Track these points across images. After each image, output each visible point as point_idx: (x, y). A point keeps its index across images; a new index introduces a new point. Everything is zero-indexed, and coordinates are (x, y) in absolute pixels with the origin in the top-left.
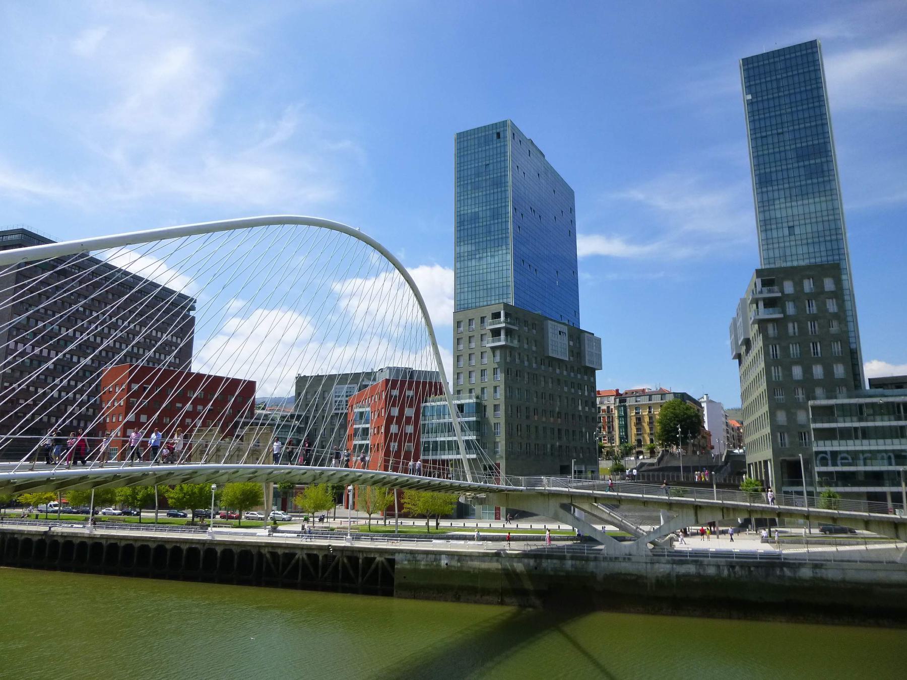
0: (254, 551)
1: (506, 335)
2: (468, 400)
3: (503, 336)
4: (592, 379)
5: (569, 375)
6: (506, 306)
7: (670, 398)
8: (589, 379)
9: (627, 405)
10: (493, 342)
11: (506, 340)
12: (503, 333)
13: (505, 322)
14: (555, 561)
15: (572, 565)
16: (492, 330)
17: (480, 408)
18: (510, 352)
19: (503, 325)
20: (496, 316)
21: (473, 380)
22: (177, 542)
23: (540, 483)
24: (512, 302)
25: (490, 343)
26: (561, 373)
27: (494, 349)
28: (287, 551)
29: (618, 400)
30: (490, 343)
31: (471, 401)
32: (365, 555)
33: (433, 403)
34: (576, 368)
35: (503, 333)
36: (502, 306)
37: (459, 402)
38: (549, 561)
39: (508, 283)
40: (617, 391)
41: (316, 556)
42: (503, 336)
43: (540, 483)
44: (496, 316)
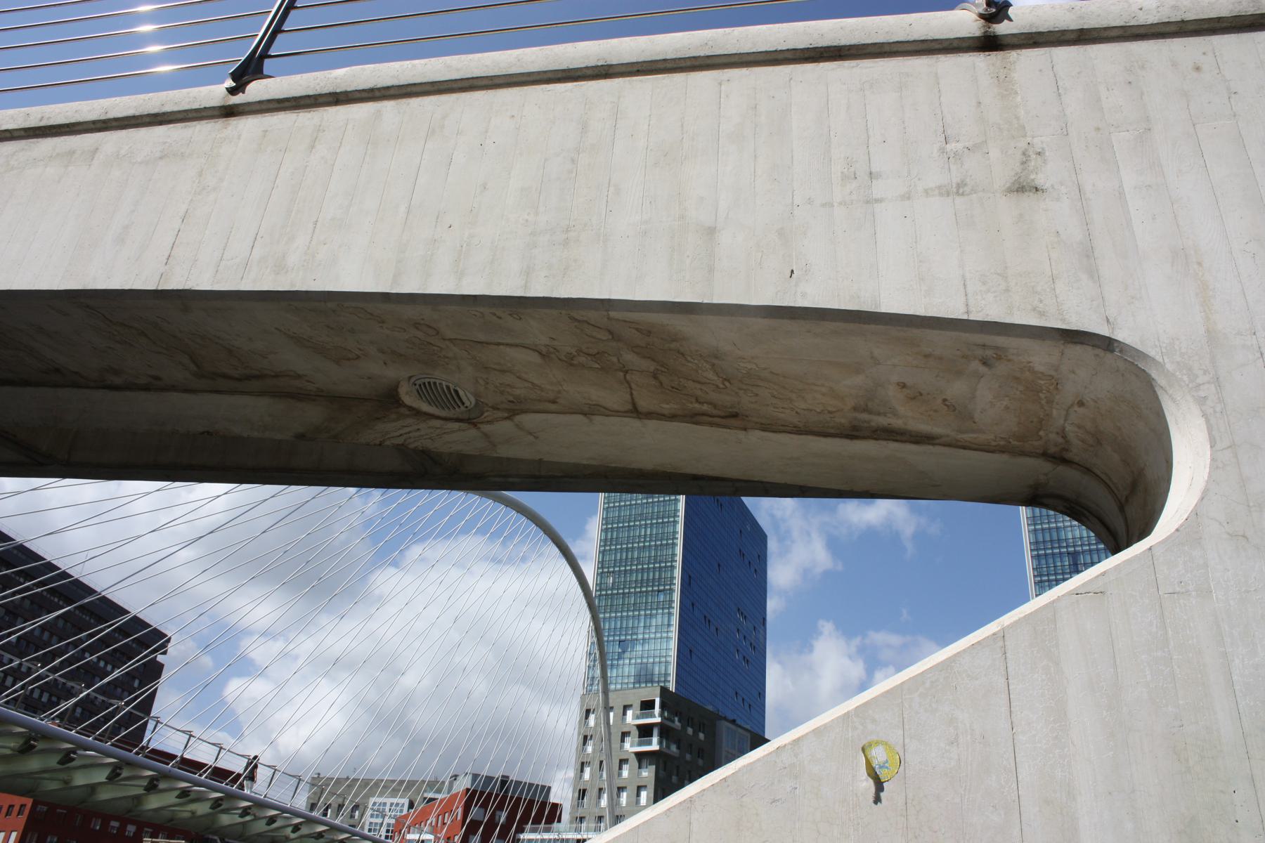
1: (661, 735)
3: (655, 739)
6: (664, 691)
10: (640, 744)
11: (660, 743)
12: (656, 732)
13: (661, 715)
16: (639, 727)
18: (665, 764)
19: (658, 720)
20: (647, 705)
24: (672, 687)
25: (631, 746)
27: (640, 756)
30: (631, 746)
35: (656, 732)
36: (658, 691)
39: (668, 659)
42: (655, 739)
44: (647, 705)
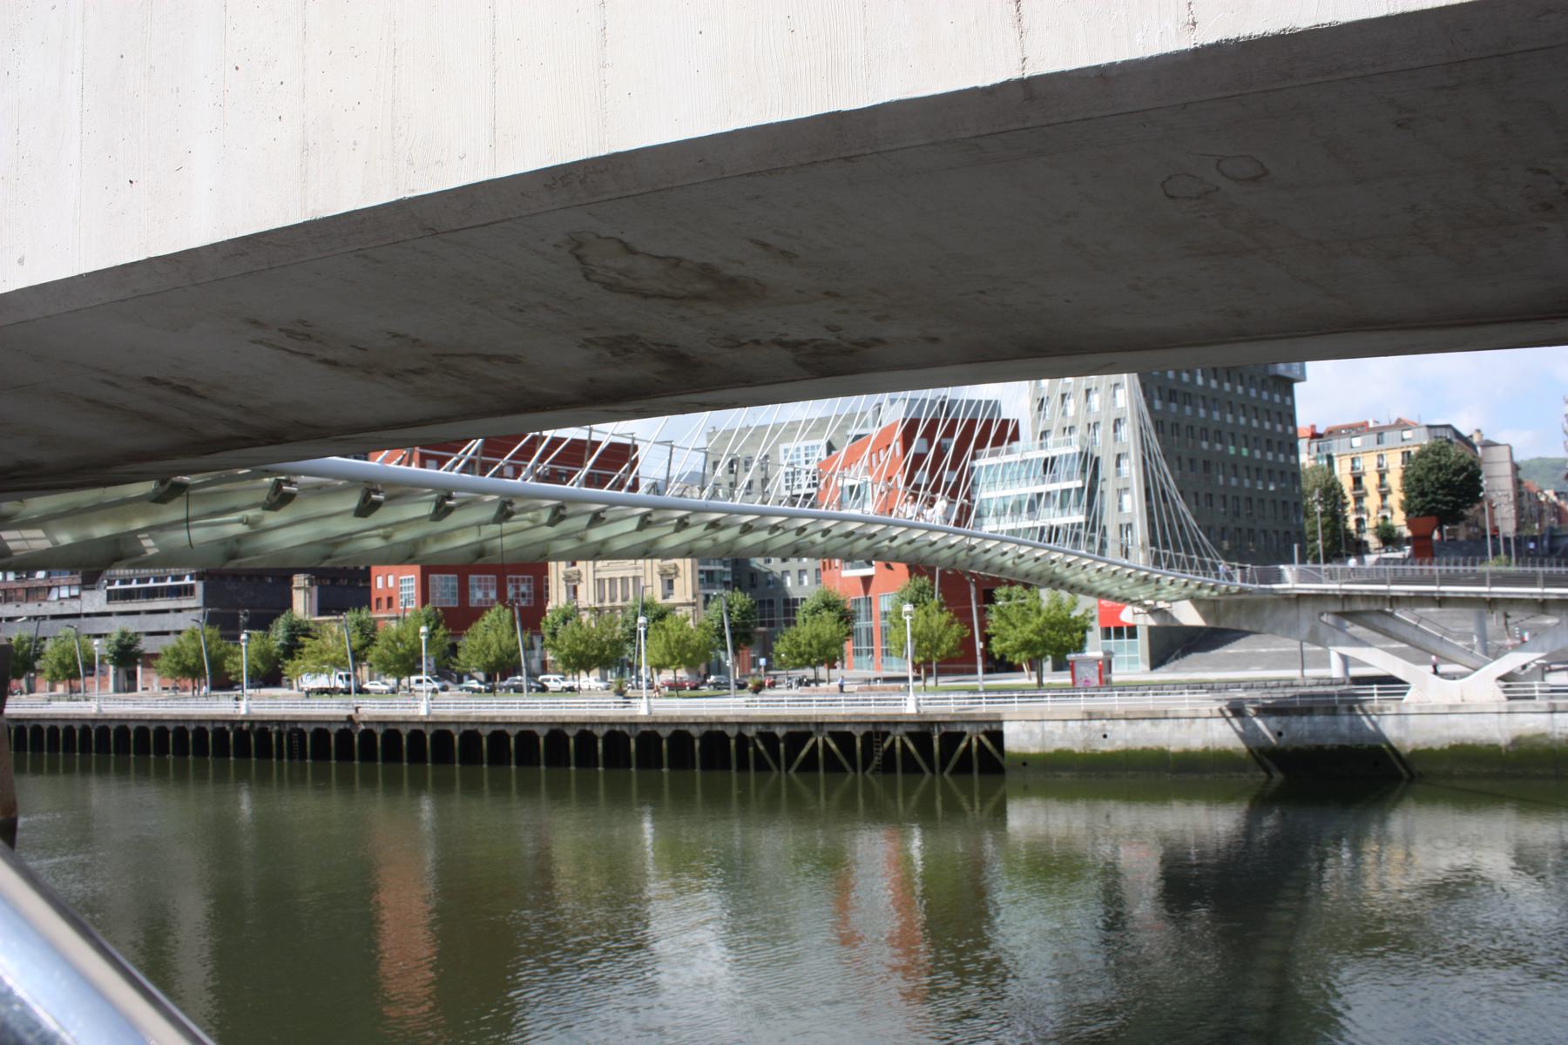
0: (732, 732)
2: (1064, 448)
4: (1288, 401)
5: (1246, 392)
7: (1418, 440)
8: (1283, 400)
9: (1334, 454)
14: (1318, 719)
15: (1352, 725)
17: (1090, 464)
21: (1071, 410)
22: (585, 724)
23: (1279, 578)
26: (1234, 390)
28: (791, 729)
29: (1314, 446)
31: (1070, 450)
32: (943, 729)
33: (985, 461)
34: (1259, 380)
37: (1044, 454)
38: (1305, 719)
40: (1313, 427)
41: (850, 737)
43: (1279, 578)
